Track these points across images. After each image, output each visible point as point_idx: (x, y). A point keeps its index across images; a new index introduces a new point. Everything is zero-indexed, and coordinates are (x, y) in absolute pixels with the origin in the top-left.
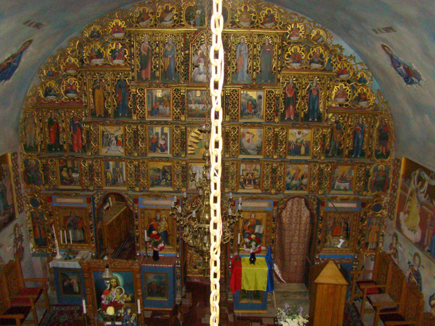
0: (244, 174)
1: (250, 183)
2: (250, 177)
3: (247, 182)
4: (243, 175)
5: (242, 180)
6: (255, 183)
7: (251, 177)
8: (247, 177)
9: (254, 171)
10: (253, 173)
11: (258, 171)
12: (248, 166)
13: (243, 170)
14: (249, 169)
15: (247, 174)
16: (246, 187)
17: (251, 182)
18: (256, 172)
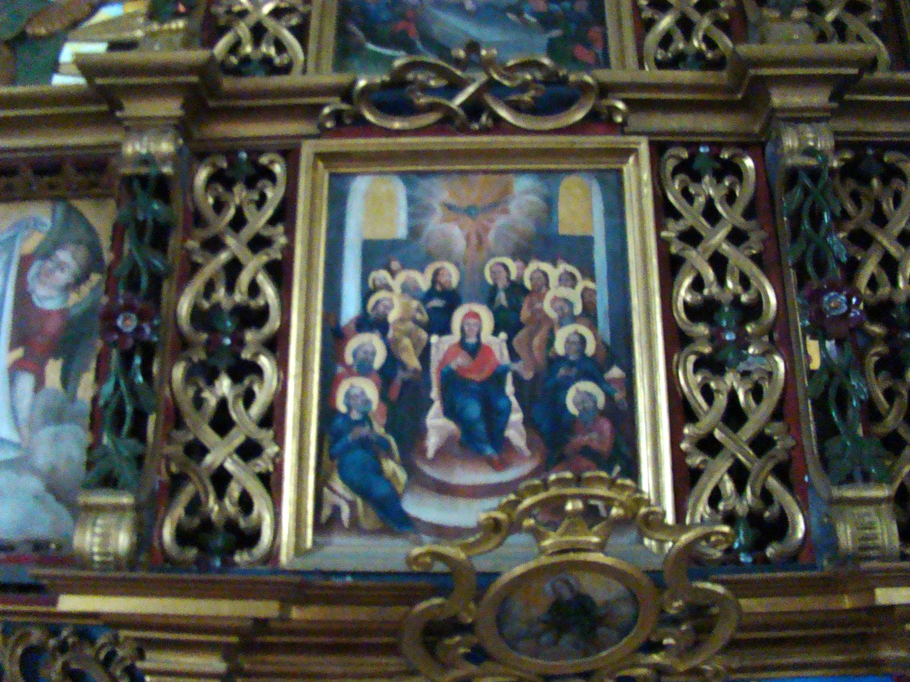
0: (396, 308)
1: (480, 437)
2: (475, 350)
3: (437, 425)
4: (365, 323)
5: (370, 389)
6: (554, 435)
7: (497, 345)
8: (440, 345)
9: (523, 254)
10: (516, 289)
11: (578, 251)
12: (441, 192)
13: (376, 254)
14: (456, 235)
15: (439, 309)
16: (422, 508)
17: (495, 418)
18: (554, 272)
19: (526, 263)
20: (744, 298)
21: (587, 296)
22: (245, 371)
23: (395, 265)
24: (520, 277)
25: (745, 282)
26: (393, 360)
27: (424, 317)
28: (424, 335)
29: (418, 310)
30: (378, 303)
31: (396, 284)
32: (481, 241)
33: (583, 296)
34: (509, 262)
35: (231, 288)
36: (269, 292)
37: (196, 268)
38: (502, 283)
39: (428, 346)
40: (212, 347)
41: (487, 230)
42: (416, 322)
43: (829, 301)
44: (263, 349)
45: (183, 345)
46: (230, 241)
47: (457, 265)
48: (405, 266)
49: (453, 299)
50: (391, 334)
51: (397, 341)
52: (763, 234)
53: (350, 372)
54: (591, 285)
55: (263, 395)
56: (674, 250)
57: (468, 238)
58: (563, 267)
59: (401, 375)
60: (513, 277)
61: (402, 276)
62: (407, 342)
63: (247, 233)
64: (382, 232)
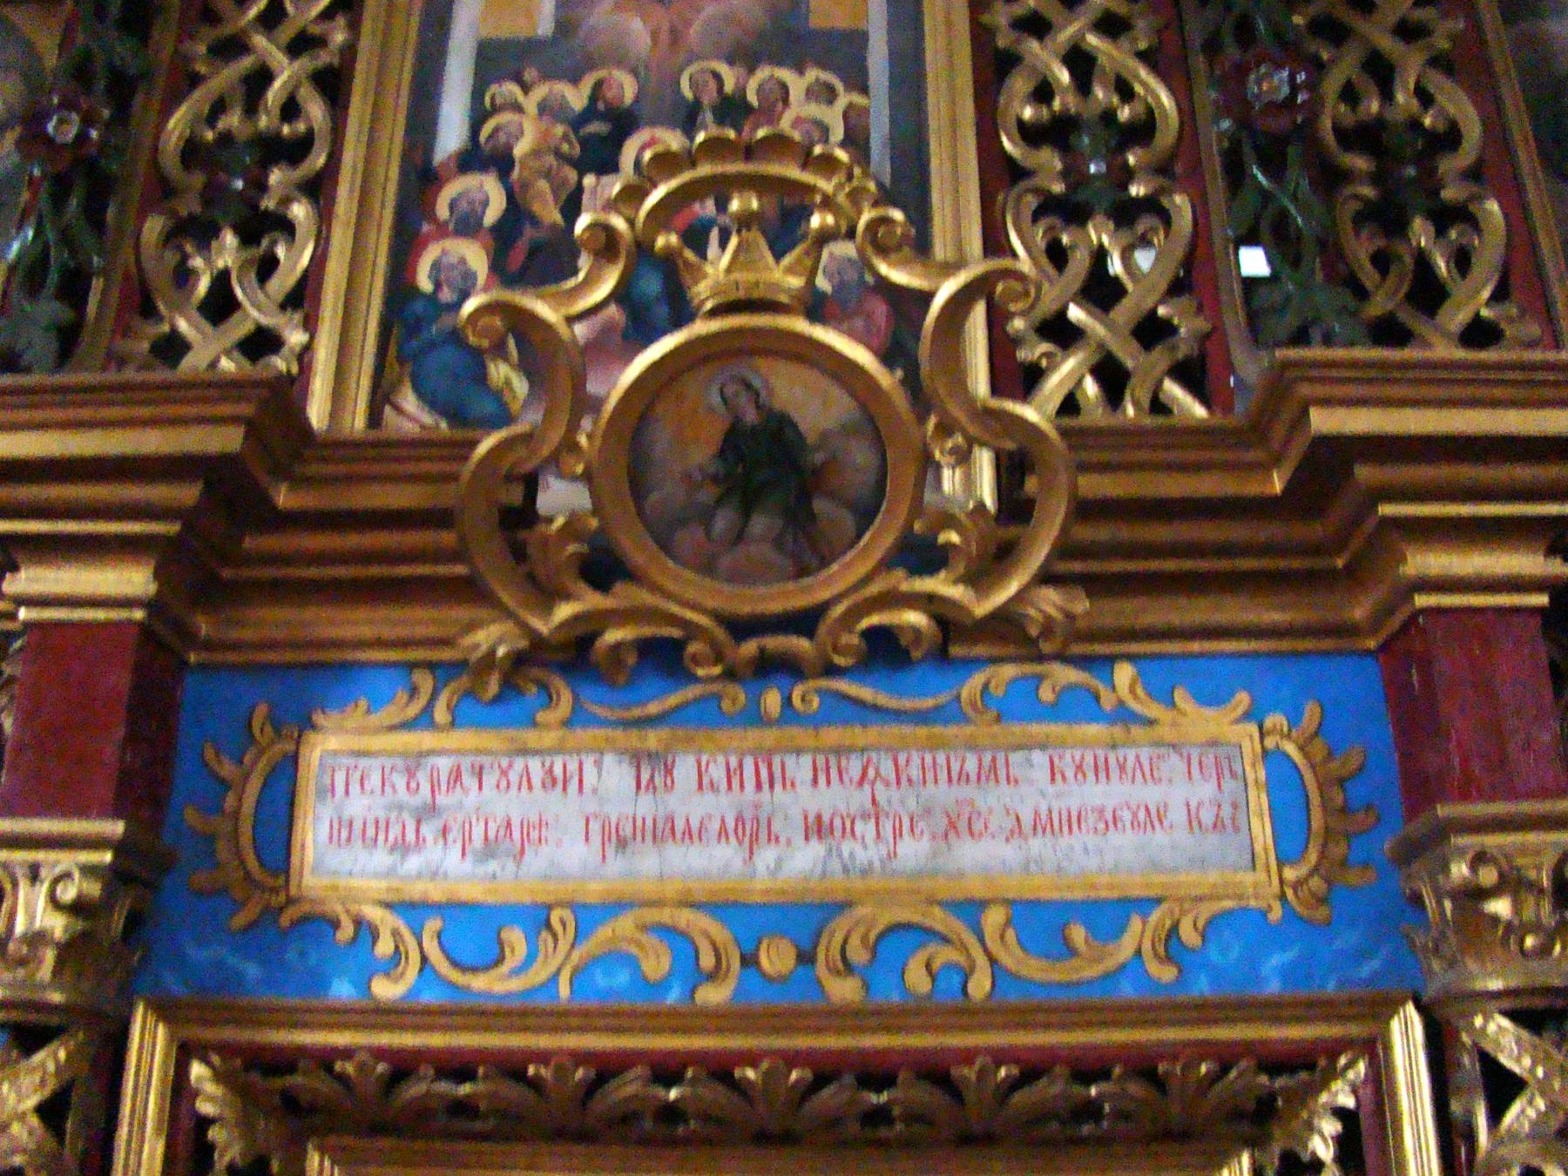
4: (471, 159)
9: (747, 56)
13: (497, 60)
18: (797, 84)
19: (751, 70)
20: (1124, 114)
21: (852, 114)
22: (262, 227)
23: (529, 74)
24: (741, 90)
25: (1125, 91)
26: (517, 212)
27: (572, 149)
28: (572, 175)
29: (565, 138)
30: (497, 130)
31: (531, 103)
32: (676, 37)
33: (845, 115)
34: (723, 69)
35: (252, 108)
36: (316, 111)
37: (195, 80)
38: (709, 97)
39: (579, 189)
40: (213, 194)
41: (688, 24)
42: (558, 154)
43: (1259, 82)
44: (296, 193)
45: (162, 190)
46: (259, 40)
47: (634, 72)
48: (547, 76)
49: (624, 123)
50: (515, 174)
51: (526, 185)
52: (1158, 22)
53: (442, 231)
54: (858, 99)
55: (294, 259)
56: (1002, 42)
57: (655, 36)
58: (813, 74)
59: (529, 233)
60: (729, 87)
61: (540, 92)
62: (543, 185)
63: (287, 32)
64: (510, 28)
